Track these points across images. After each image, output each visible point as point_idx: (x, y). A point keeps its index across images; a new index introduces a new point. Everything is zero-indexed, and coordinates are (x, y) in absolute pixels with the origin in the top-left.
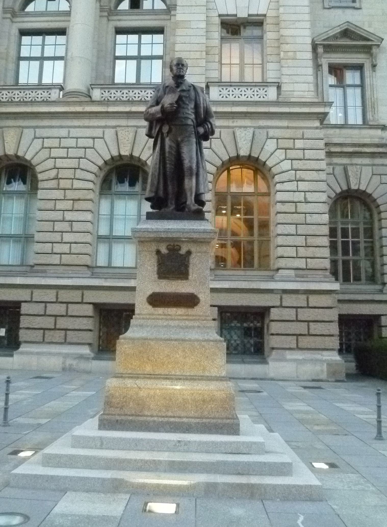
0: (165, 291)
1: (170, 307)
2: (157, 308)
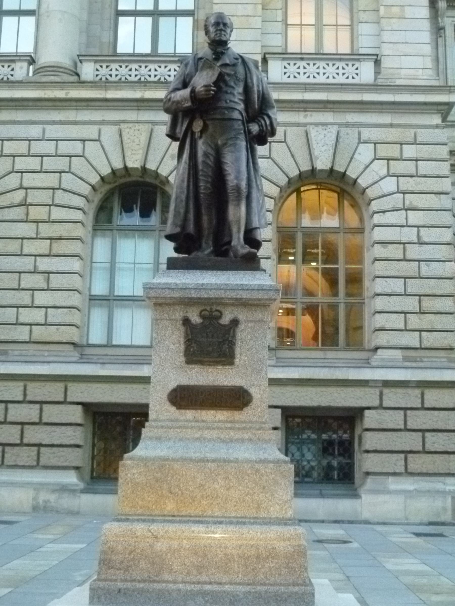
0: (196, 383)
1: (204, 409)
2: (183, 411)
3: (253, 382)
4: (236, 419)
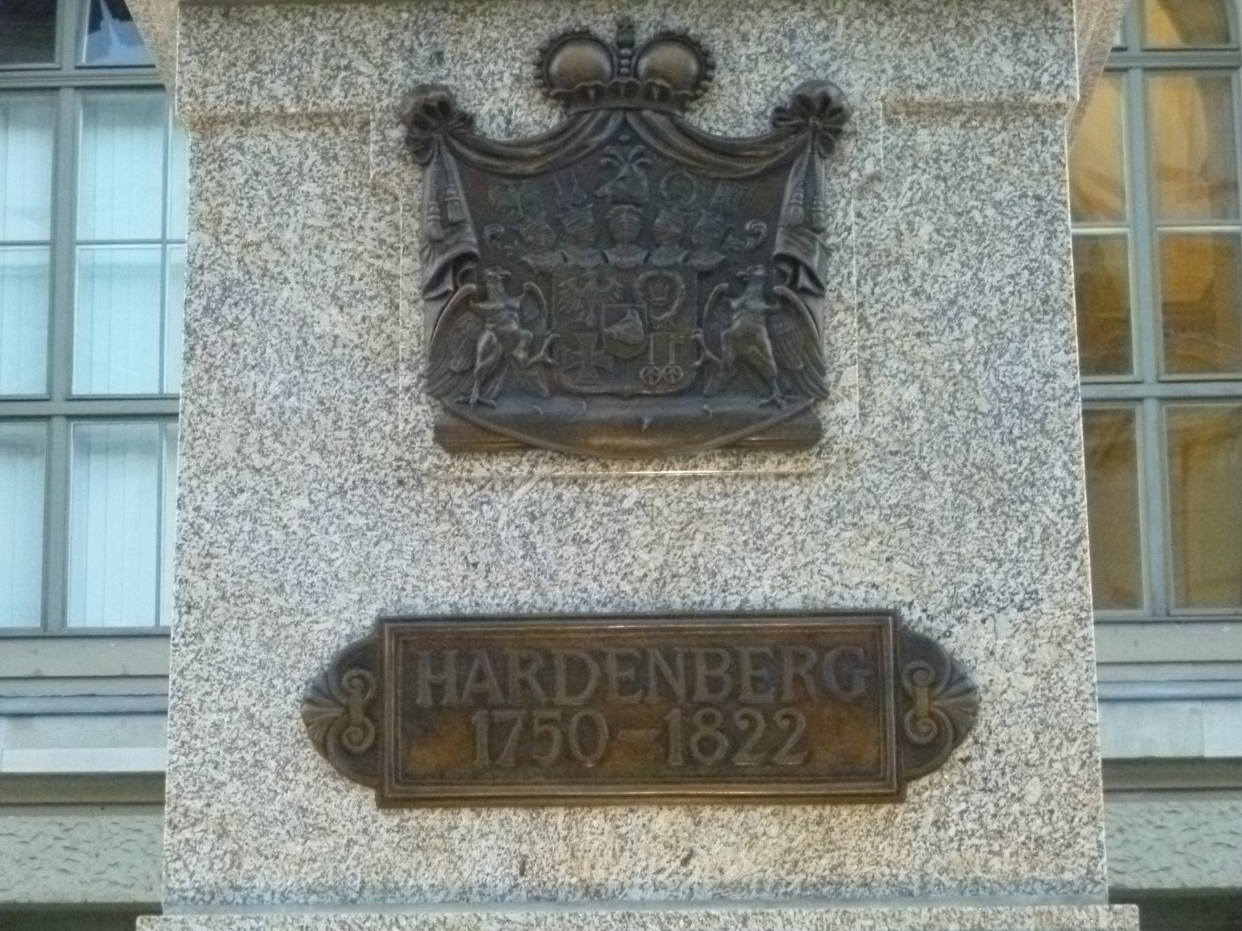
0: (526, 599)
1: (589, 802)
2: (434, 818)
3: (973, 578)
4: (851, 868)
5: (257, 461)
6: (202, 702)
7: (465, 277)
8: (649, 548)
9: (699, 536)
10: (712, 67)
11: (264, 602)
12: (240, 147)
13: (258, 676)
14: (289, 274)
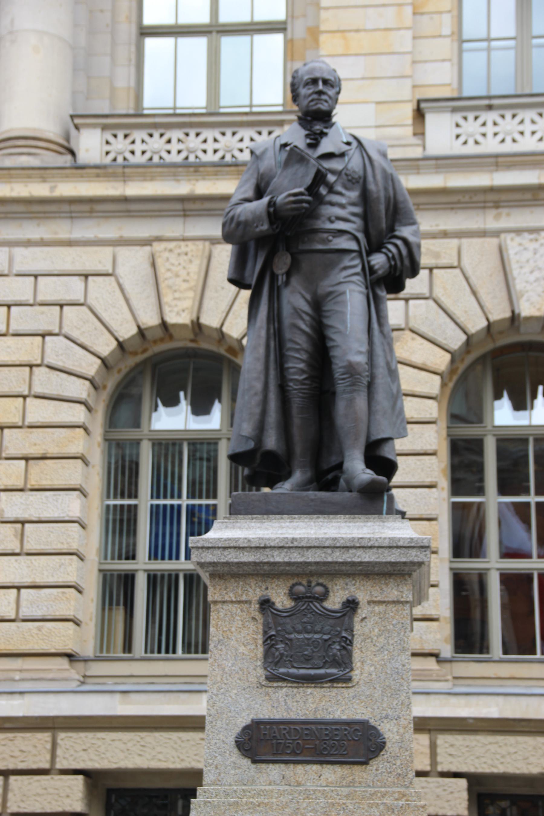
3: (385, 712)
4: (357, 779)
5: (226, 681)
6: (212, 737)
7: (272, 640)
8: (313, 703)
9: (324, 701)
10: (328, 591)
11: (227, 715)
12: (222, 608)
13: (225, 732)
14: (233, 638)
